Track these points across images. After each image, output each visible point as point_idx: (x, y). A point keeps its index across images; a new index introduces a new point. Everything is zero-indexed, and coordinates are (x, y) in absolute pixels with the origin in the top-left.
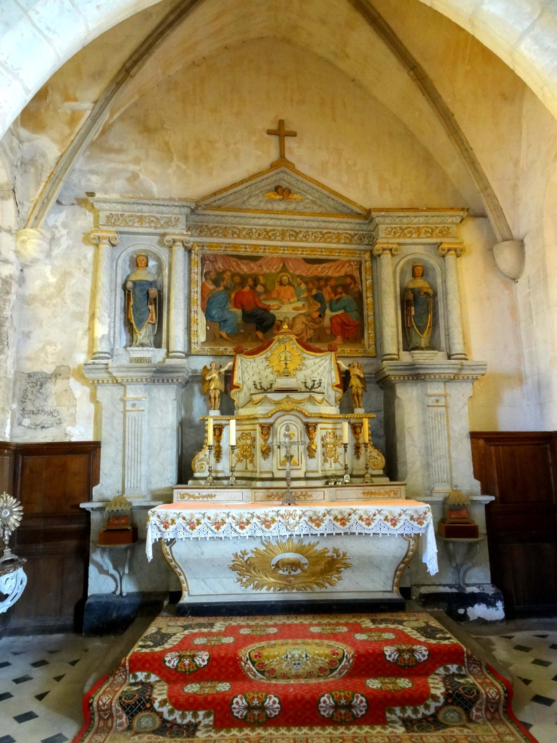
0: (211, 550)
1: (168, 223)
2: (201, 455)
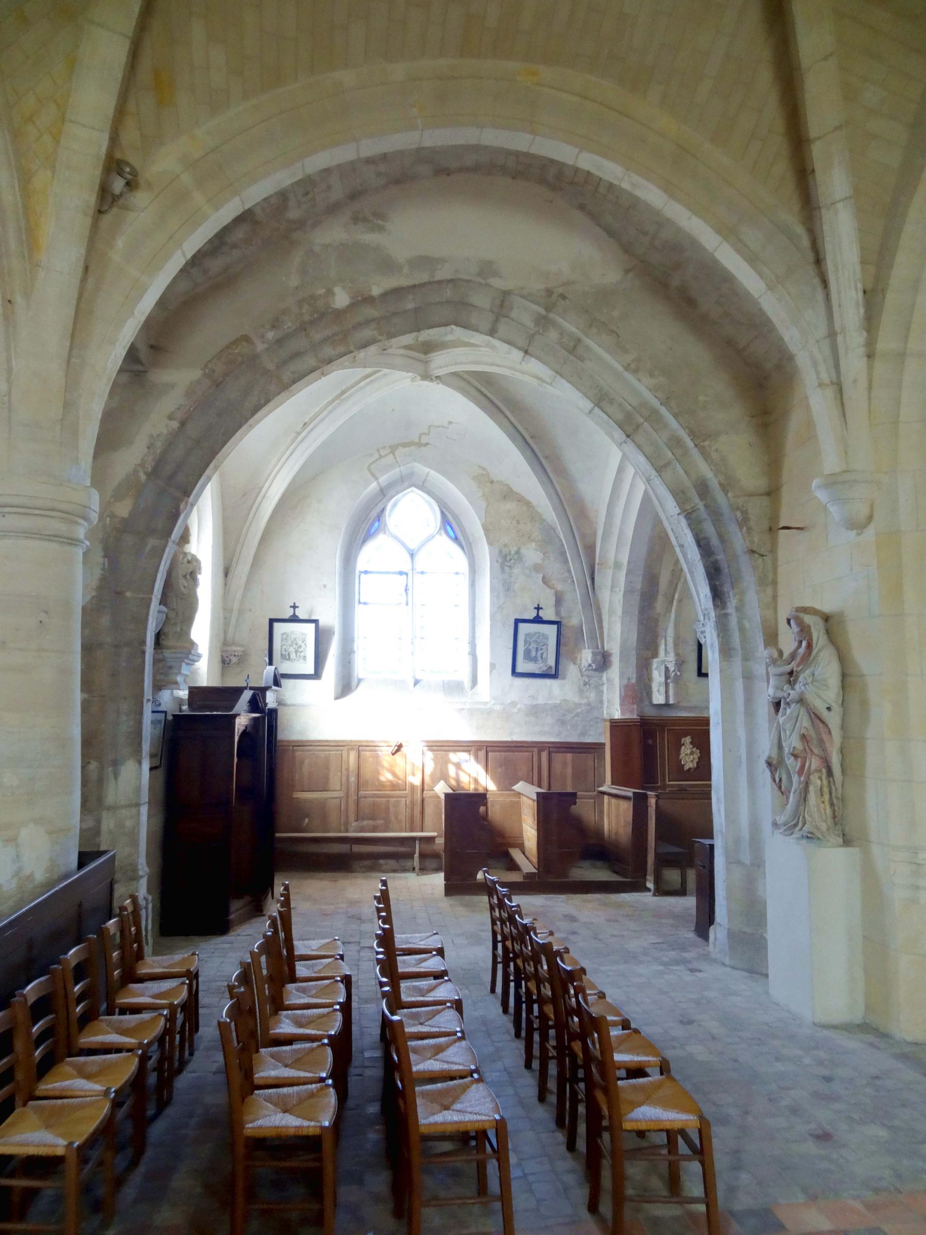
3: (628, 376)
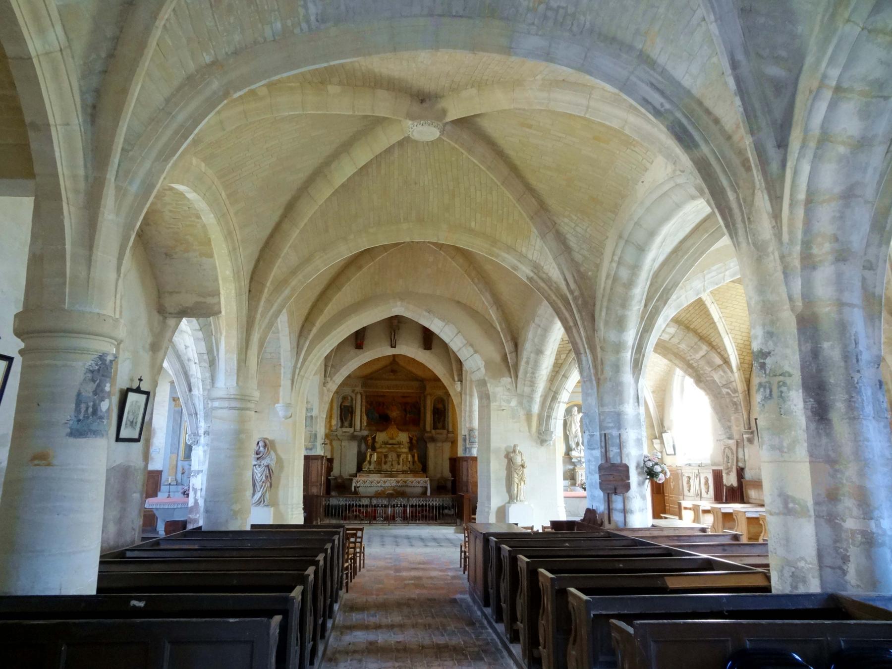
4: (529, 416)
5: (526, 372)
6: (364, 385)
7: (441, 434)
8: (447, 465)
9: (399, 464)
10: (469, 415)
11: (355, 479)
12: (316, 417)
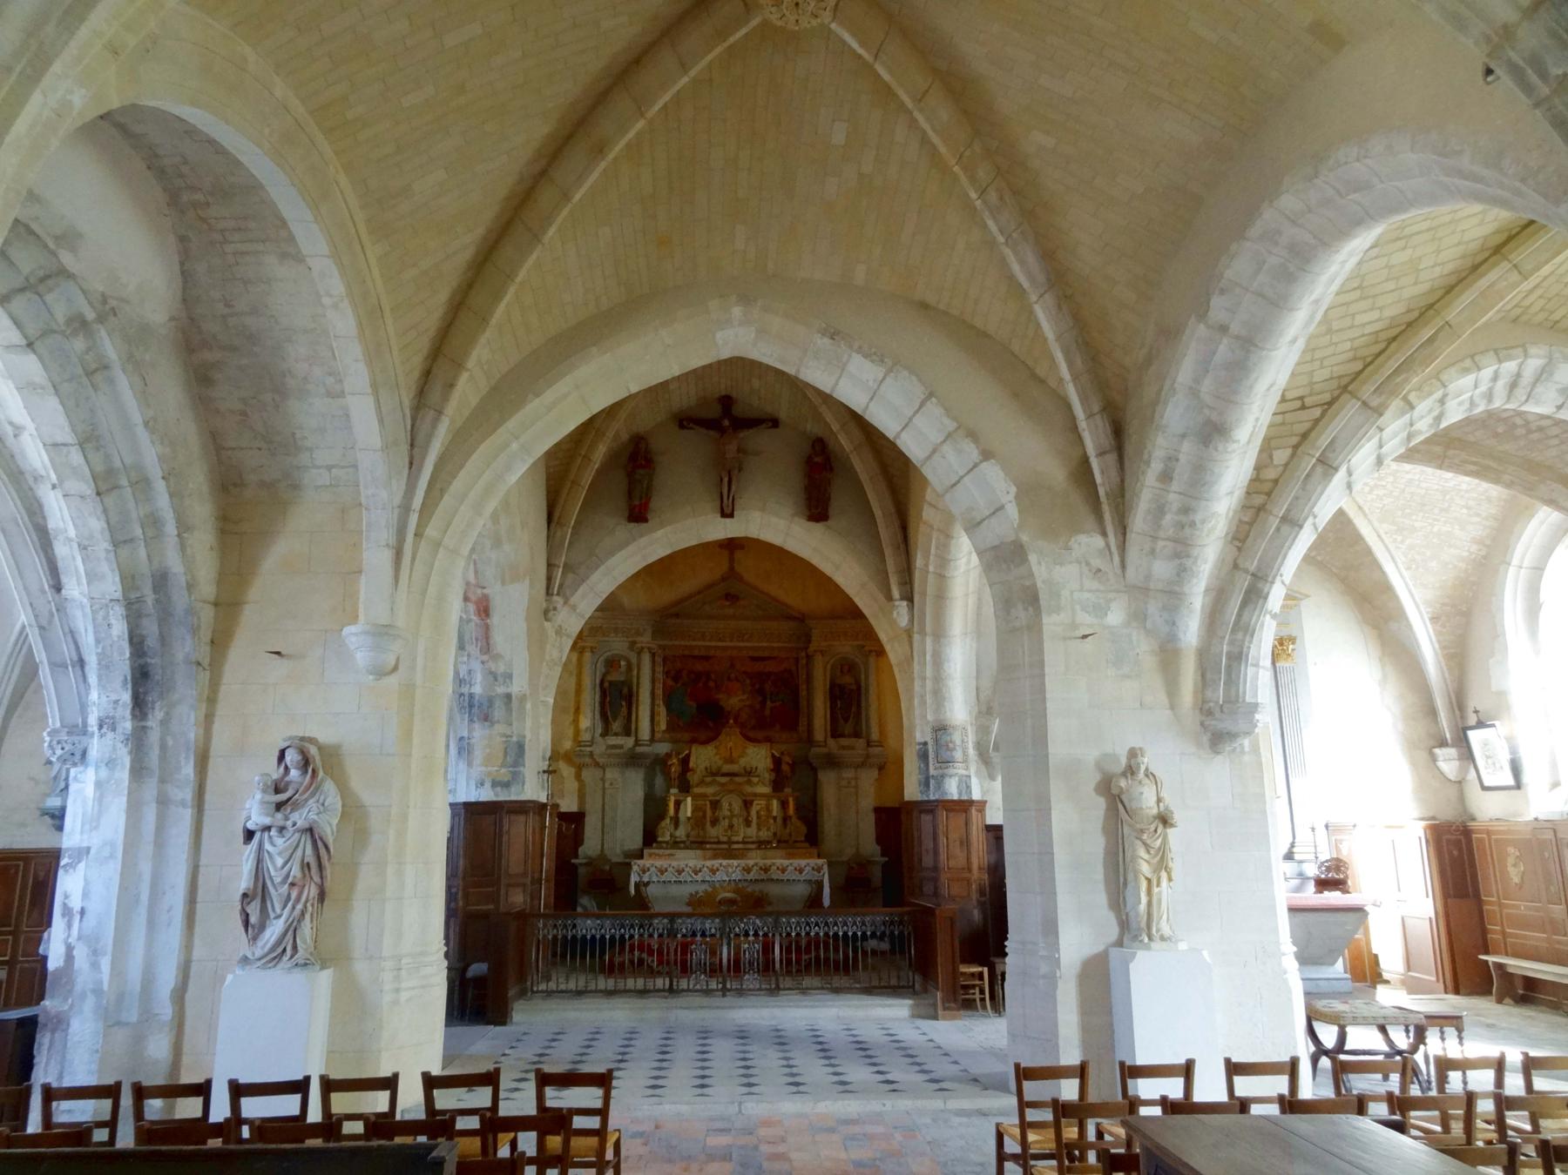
0: (675, 890)
1: (638, 633)
2: (663, 824)
3: (143, 435)
4: (1168, 655)
5: (1159, 510)
6: (658, 632)
7: (853, 748)
8: (868, 827)
9: (748, 823)
10: (949, 678)
11: (637, 865)
12: (523, 699)
